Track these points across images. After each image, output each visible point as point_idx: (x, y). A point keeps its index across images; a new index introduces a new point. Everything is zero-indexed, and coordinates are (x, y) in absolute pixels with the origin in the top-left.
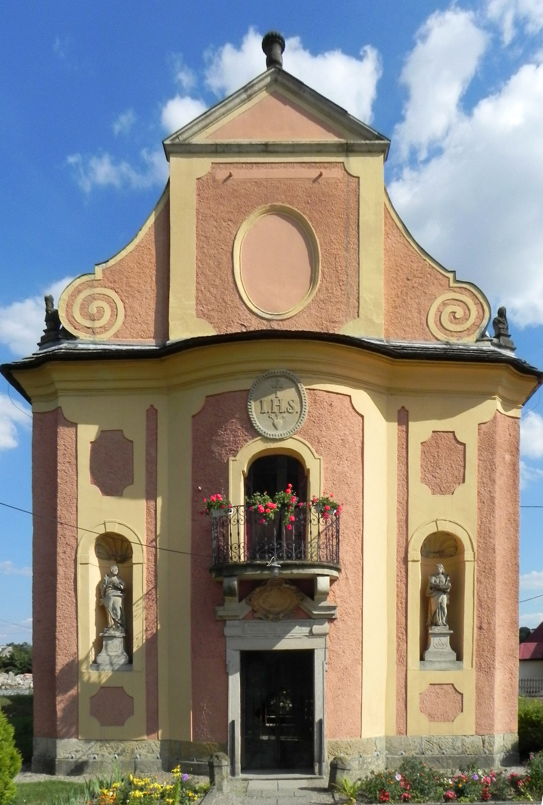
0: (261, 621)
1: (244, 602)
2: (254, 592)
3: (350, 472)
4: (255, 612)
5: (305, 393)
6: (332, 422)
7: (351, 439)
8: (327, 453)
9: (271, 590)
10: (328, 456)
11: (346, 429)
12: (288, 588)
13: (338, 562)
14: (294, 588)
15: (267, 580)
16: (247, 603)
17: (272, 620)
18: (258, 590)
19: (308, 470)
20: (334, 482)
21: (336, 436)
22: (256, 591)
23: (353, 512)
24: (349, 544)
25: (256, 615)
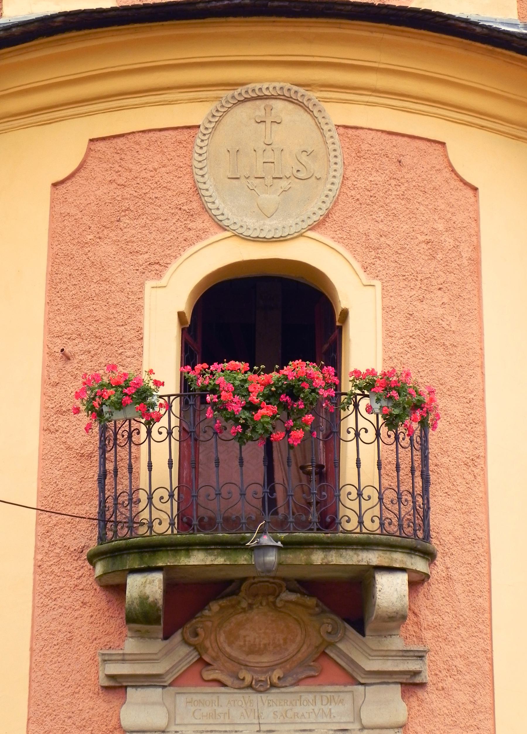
0: (223, 689)
1: (177, 637)
2: (206, 612)
3: (450, 318)
4: (208, 664)
5: (336, 136)
6: (403, 202)
7: (449, 242)
8: (391, 272)
9: (250, 606)
10: (395, 279)
11: (436, 218)
12: (296, 603)
13: (427, 537)
14: (311, 601)
15: (243, 580)
16: (186, 642)
17: (250, 686)
18: (215, 607)
19: (345, 313)
20: (411, 340)
21: (413, 234)
22: (210, 610)
23: (458, 414)
24: (451, 493)
25: (209, 675)
